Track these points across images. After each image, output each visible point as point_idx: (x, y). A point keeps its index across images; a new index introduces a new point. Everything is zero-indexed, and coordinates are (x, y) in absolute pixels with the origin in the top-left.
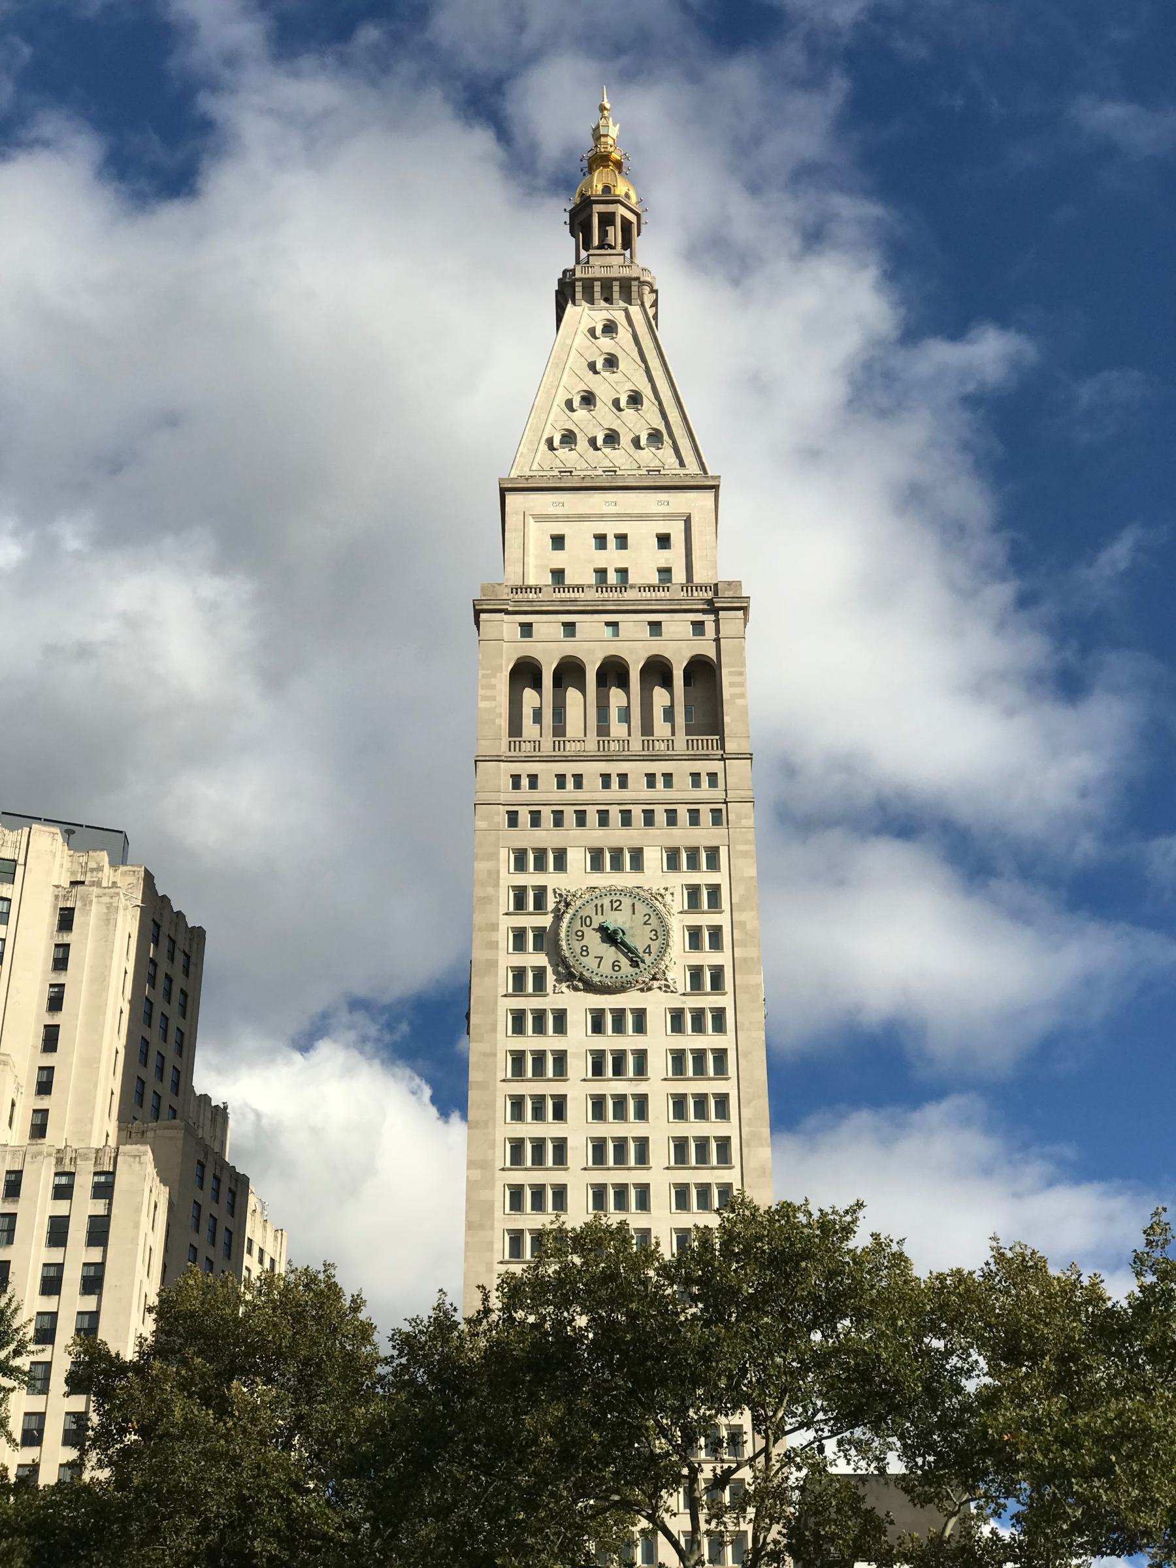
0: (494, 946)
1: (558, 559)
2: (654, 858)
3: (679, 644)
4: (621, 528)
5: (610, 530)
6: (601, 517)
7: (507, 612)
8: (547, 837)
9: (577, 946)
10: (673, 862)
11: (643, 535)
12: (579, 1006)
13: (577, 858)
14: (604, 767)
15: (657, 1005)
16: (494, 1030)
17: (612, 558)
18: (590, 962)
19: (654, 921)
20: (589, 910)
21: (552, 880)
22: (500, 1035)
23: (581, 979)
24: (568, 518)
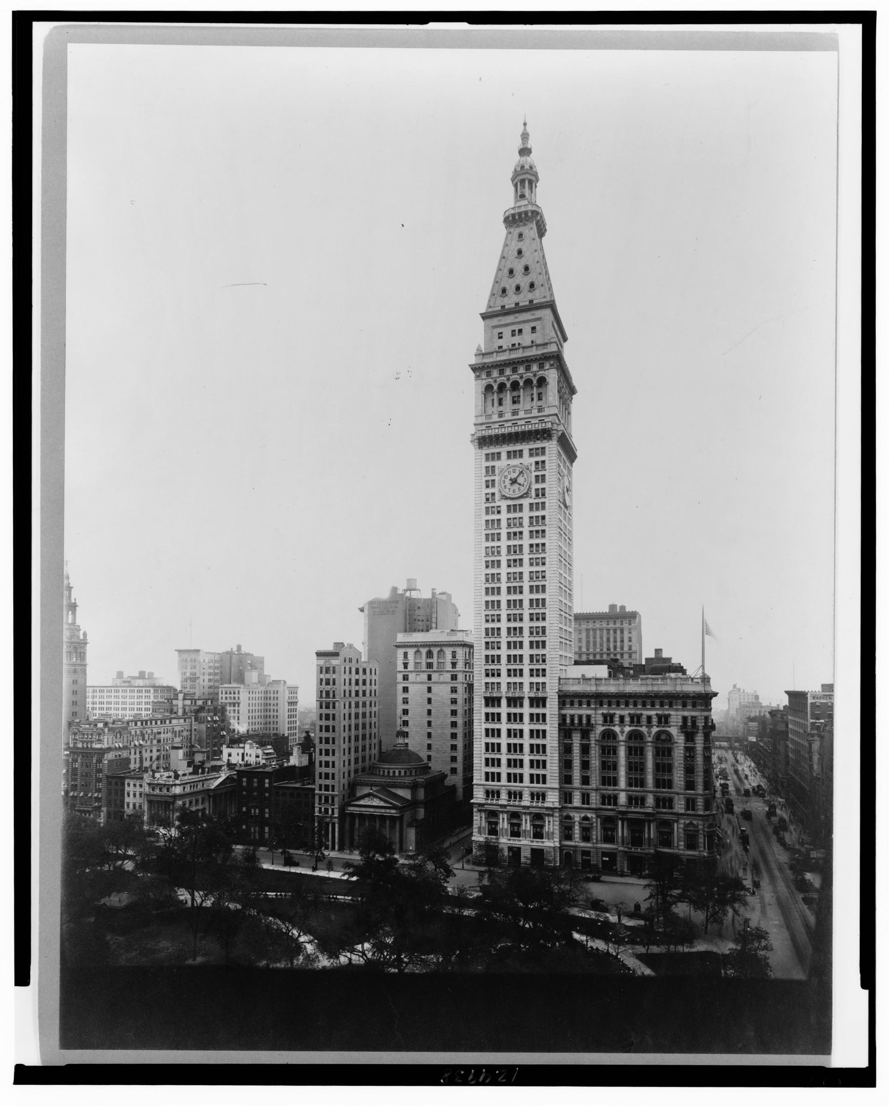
2: (526, 453)
5: (516, 328)
6: (513, 324)
10: (531, 455)
11: (527, 328)
12: (504, 504)
13: (504, 455)
15: (526, 502)
21: (497, 463)
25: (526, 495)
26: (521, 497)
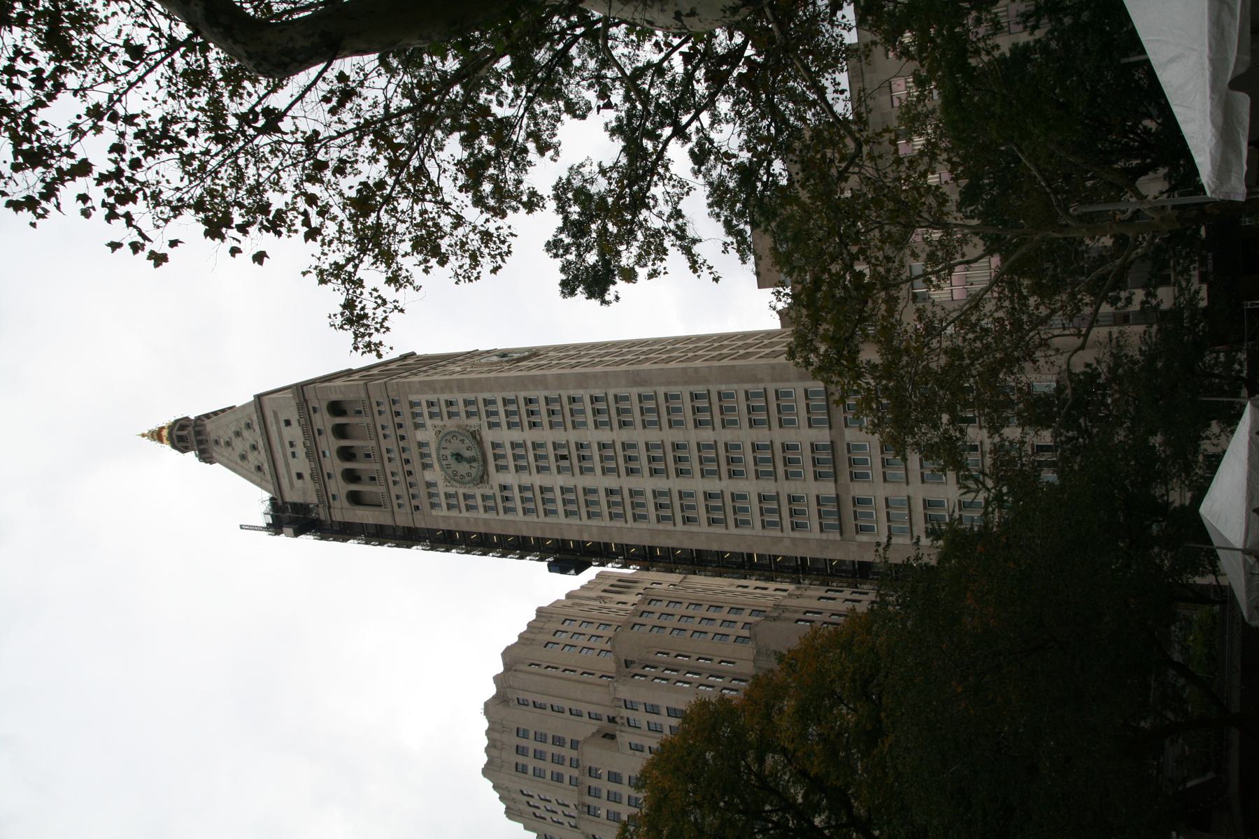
0: (476, 519)
1: (307, 476)
2: (421, 436)
3: (324, 421)
4: (288, 445)
5: (289, 450)
6: (285, 455)
7: (329, 507)
8: (423, 492)
9: (467, 479)
12: (497, 478)
13: (429, 476)
14: (386, 461)
15: (489, 436)
16: (514, 522)
17: (301, 451)
18: (474, 472)
19: (449, 437)
20: (450, 471)
21: (442, 488)
22: (517, 519)
23: (482, 477)
24: (289, 472)
25: (475, 436)
26: (480, 443)
